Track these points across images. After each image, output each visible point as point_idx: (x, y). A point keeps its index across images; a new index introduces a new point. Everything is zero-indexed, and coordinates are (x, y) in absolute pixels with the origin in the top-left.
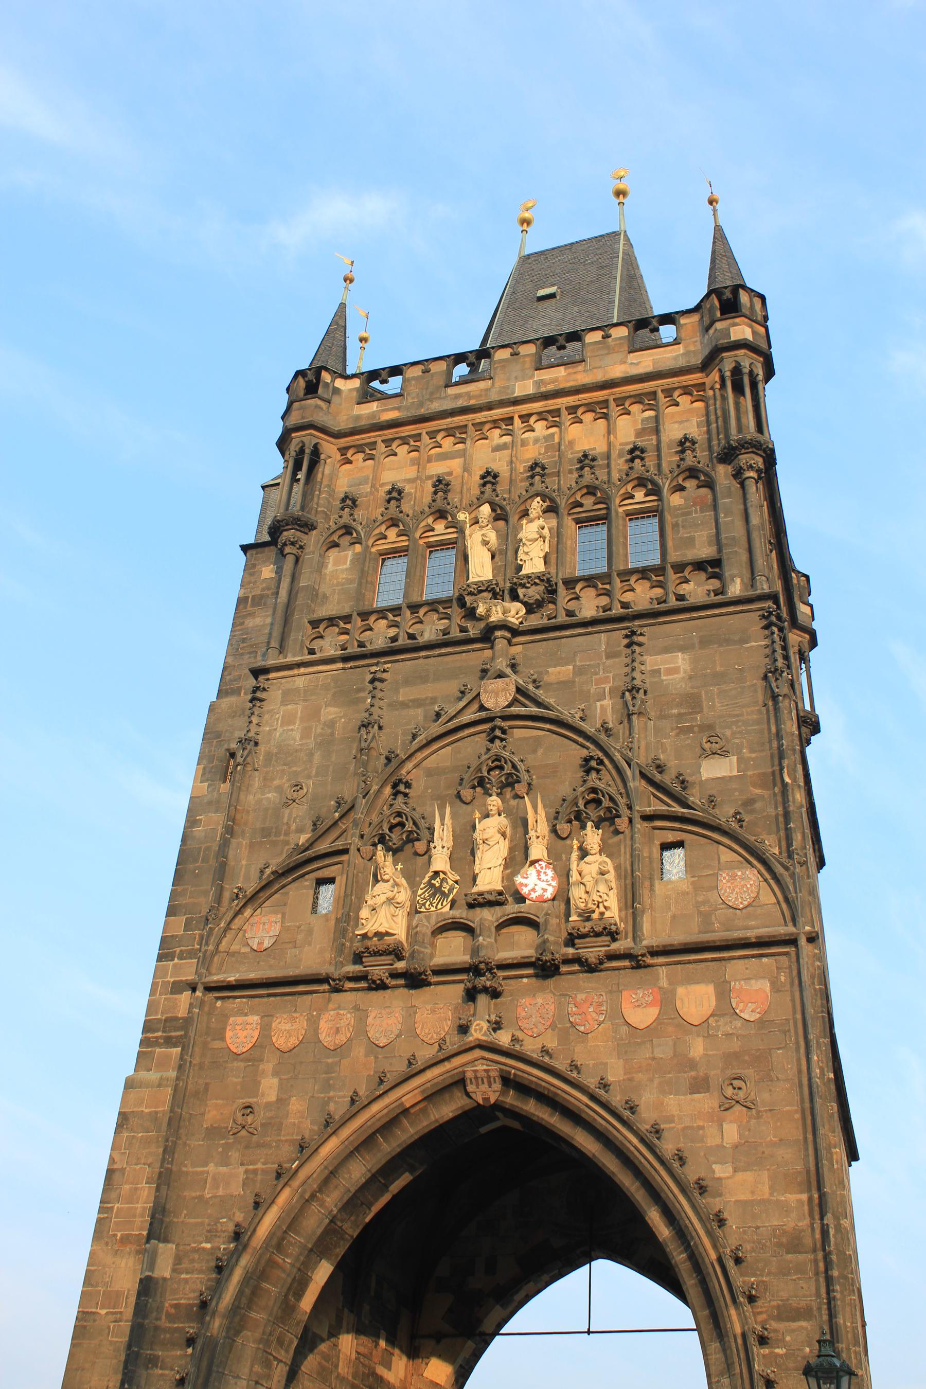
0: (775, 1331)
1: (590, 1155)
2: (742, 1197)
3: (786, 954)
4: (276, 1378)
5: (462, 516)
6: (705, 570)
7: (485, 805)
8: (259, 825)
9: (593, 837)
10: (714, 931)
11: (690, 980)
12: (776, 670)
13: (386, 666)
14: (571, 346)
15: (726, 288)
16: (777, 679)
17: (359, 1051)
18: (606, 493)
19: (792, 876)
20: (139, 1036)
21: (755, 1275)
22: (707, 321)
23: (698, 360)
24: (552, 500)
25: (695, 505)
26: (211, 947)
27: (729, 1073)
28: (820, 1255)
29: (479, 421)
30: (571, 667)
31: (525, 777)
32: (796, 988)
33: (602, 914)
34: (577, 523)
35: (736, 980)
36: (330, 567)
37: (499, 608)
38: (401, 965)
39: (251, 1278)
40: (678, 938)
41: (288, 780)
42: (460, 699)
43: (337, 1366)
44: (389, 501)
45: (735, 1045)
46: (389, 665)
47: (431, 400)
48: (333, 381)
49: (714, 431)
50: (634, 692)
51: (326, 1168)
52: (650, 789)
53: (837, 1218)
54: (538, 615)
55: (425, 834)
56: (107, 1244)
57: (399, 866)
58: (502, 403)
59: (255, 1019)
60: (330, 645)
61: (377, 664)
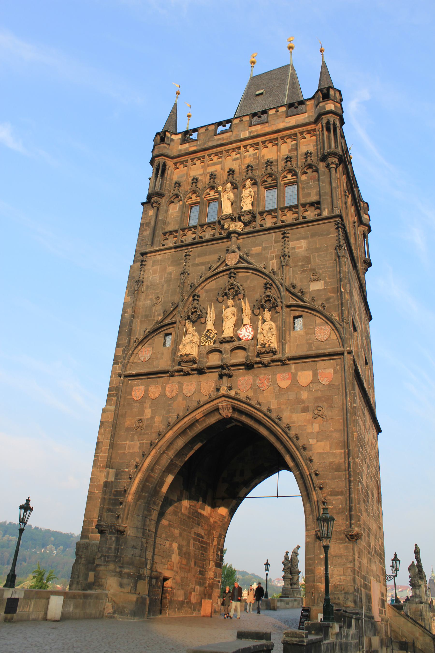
0: (329, 500)
1: (265, 436)
2: (319, 451)
3: (340, 358)
4: (153, 516)
5: (220, 188)
6: (314, 206)
7: (227, 303)
8: (144, 314)
9: (267, 315)
10: (313, 350)
11: (303, 369)
12: (340, 246)
13: (191, 250)
14: (264, 117)
15: (324, 88)
16: (340, 250)
17: (180, 399)
18: (276, 176)
19: (343, 328)
20: (107, 393)
21: (323, 480)
22: (317, 103)
23: (312, 119)
24: (255, 180)
25: (311, 179)
26: (126, 361)
27: (316, 405)
28: (347, 472)
29: (227, 149)
30: (261, 247)
31: (242, 292)
32: (343, 372)
33: (269, 345)
34: (265, 189)
35: (320, 369)
36: (171, 211)
37: (233, 225)
38: (195, 366)
39: (142, 481)
40: (299, 353)
41: (155, 296)
42: (218, 262)
43: (181, 510)
44: (192, 183)
45: (319, 394)
46: (192, 249)
47: (209, 142)
48: (171, 136)
49: (319, 149)
50: (285, 256)
51: (168, 442)
52: (290, 295)
53: (354, 459)
54: (249, 227)
55: (204, 315)
56: (97, 468)
57: (194, 328)
58: (236, 141)
59: (143, 387)
60: (170, 242)
61: (187, 249)
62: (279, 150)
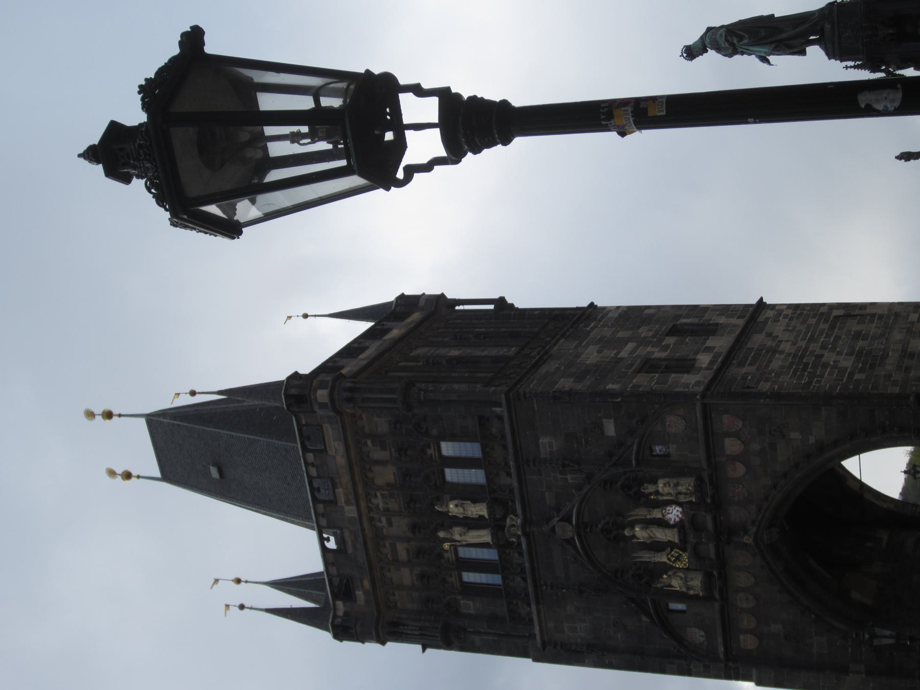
36: (472, 612)
48: (340, 617)
59: (741, 636)
62: (382, 463)
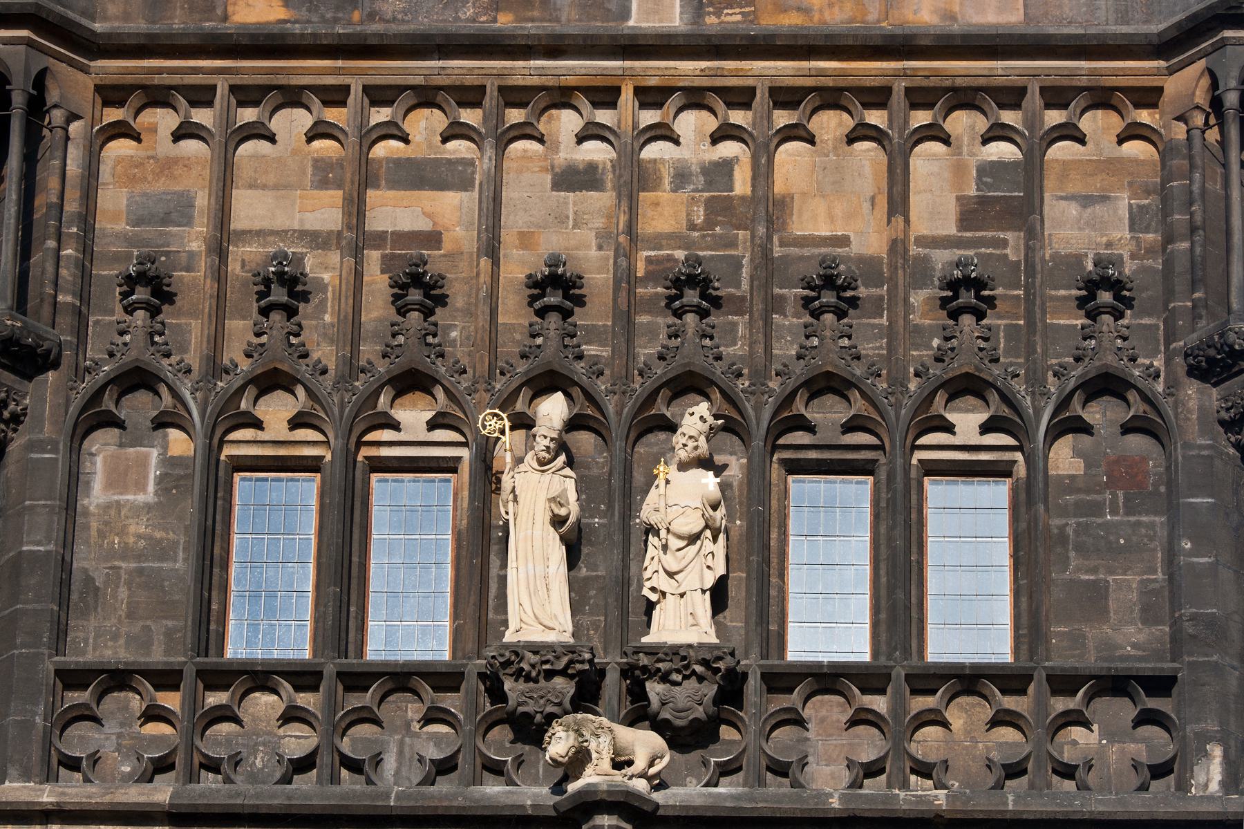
25: (1112, 484)
29: (519, 81)
36: (97, 495)
